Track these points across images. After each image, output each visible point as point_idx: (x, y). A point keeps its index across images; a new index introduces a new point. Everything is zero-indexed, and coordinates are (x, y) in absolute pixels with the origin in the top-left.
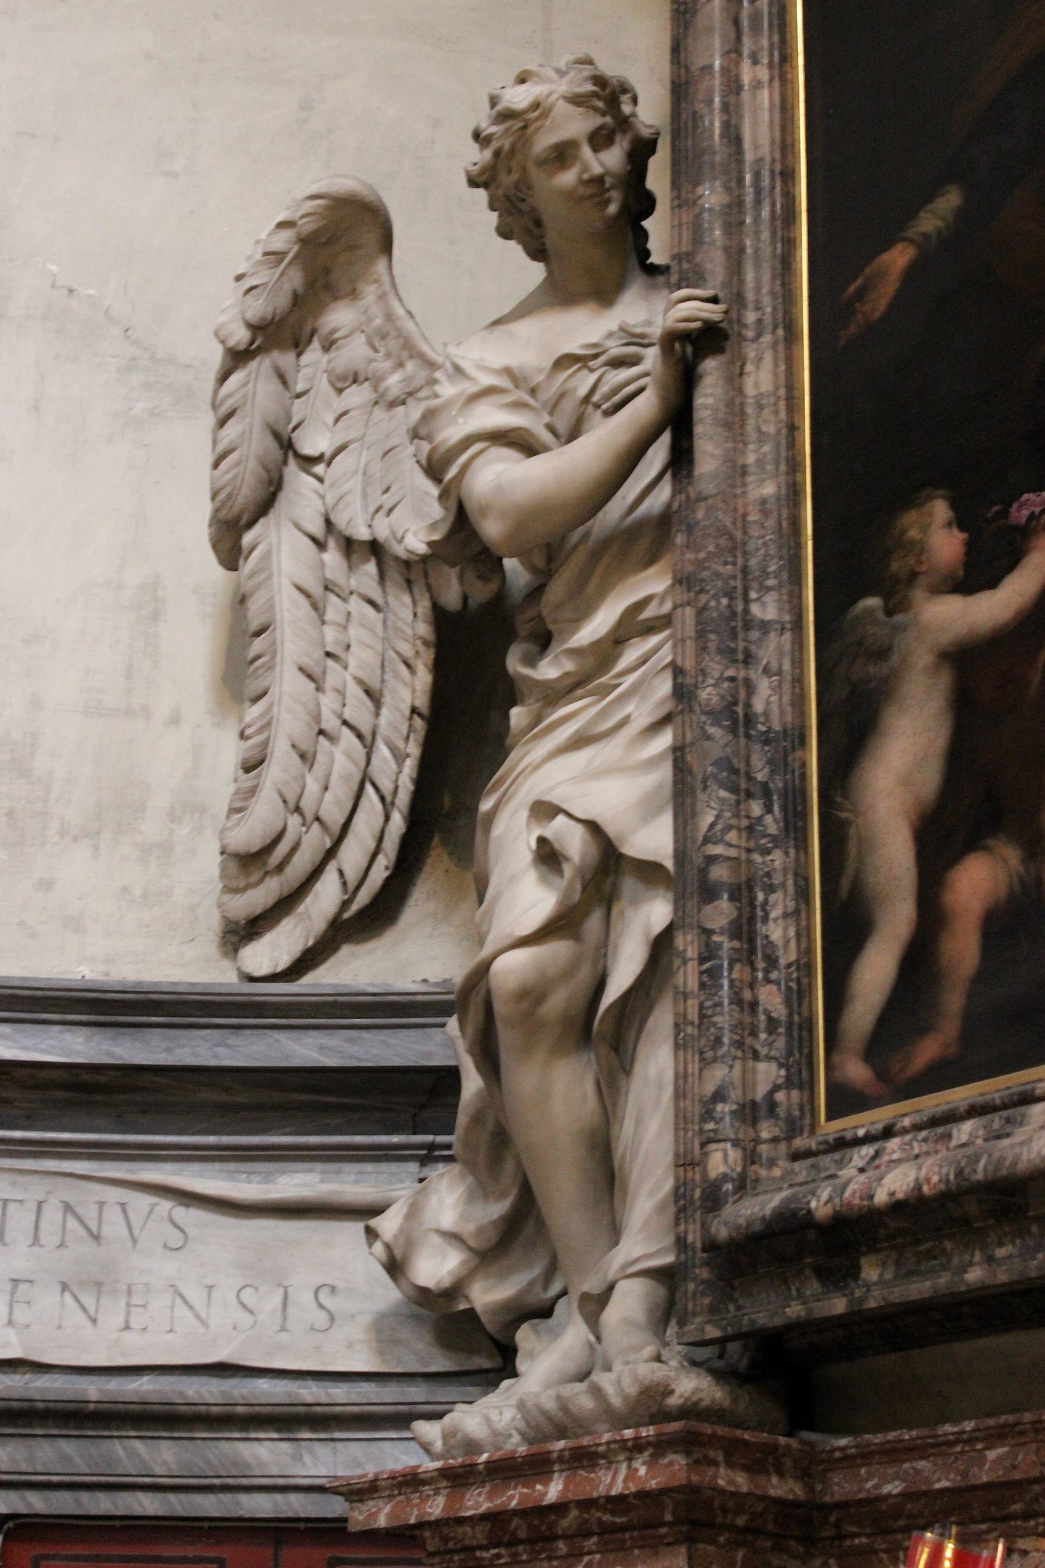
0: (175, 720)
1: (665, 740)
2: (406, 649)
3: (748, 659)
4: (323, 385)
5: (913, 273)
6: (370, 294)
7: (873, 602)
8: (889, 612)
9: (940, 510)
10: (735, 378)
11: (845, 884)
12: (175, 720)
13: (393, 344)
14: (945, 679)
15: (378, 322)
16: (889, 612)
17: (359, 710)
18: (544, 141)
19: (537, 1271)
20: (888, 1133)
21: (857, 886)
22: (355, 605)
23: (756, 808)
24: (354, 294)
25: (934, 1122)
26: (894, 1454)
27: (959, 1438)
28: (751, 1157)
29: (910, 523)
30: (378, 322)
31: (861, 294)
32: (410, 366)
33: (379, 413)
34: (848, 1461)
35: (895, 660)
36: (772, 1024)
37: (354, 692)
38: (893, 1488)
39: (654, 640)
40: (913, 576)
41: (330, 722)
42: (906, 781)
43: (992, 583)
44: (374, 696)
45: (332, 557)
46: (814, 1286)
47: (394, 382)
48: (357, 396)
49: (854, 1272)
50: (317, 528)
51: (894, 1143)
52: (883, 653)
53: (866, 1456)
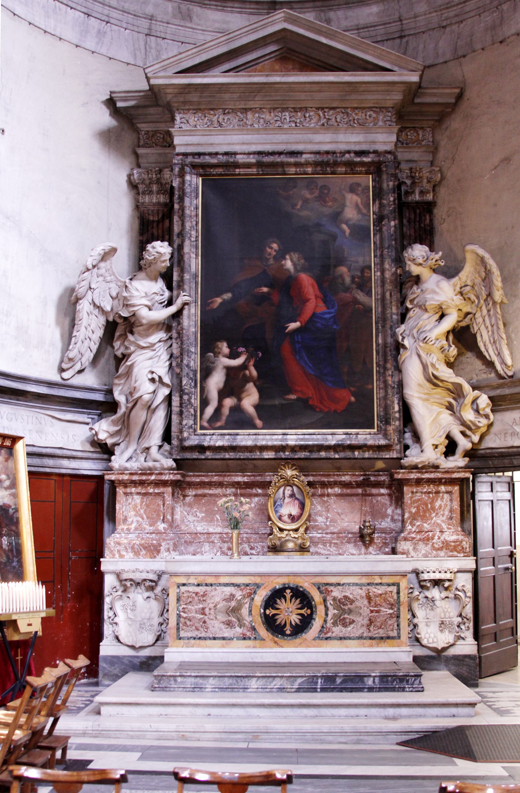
0: (49, 327)
1: (168, 363)
2: (100, 326)
3: (190, 357)
4: (96, 276)
5: (221, 304)
6: (108, 262)
7: (212, 354)
8: (215, 357)
9: (225, 344)
10: (189, 310)
11: (204, 396)
12: (49, 327)
13: (110, 272)
14: (224, 371)
15: (109, 267)
16: (215, 357)
17: (90, 334)
18: (163, 259)
19: (118, 438)
20: (213, 435)
21: (206, 397)
22: (94, 316)
23: (190, 381)
24: (106, 261)
25: (221, 435)
26: (198, 476)
27: (212, 475)
28: (189, 434)
29: (219, 344)
30: (109, 267)
31: (211, 303)
32: (113, 277)
33: (104, 283)
34: (191, 476)
35: (215, 365)
36: (192, 415)
37: (91, 332)
38: (198, 480)
39: (161, 343)
40: (219, 353)
41: (87, 337)
42: (217, 384)
43: (234, 359)
44: (93, 332)
45: (92, 307)
46: (197, 454)
47: (108, 279)
48: (101, 279)
49: (205, 453)
50: (91, 301)
51: (214, 436)
52: (213, 363)
53: (194, 476)
